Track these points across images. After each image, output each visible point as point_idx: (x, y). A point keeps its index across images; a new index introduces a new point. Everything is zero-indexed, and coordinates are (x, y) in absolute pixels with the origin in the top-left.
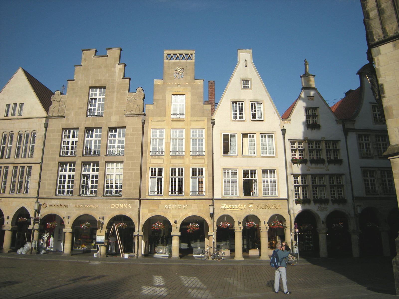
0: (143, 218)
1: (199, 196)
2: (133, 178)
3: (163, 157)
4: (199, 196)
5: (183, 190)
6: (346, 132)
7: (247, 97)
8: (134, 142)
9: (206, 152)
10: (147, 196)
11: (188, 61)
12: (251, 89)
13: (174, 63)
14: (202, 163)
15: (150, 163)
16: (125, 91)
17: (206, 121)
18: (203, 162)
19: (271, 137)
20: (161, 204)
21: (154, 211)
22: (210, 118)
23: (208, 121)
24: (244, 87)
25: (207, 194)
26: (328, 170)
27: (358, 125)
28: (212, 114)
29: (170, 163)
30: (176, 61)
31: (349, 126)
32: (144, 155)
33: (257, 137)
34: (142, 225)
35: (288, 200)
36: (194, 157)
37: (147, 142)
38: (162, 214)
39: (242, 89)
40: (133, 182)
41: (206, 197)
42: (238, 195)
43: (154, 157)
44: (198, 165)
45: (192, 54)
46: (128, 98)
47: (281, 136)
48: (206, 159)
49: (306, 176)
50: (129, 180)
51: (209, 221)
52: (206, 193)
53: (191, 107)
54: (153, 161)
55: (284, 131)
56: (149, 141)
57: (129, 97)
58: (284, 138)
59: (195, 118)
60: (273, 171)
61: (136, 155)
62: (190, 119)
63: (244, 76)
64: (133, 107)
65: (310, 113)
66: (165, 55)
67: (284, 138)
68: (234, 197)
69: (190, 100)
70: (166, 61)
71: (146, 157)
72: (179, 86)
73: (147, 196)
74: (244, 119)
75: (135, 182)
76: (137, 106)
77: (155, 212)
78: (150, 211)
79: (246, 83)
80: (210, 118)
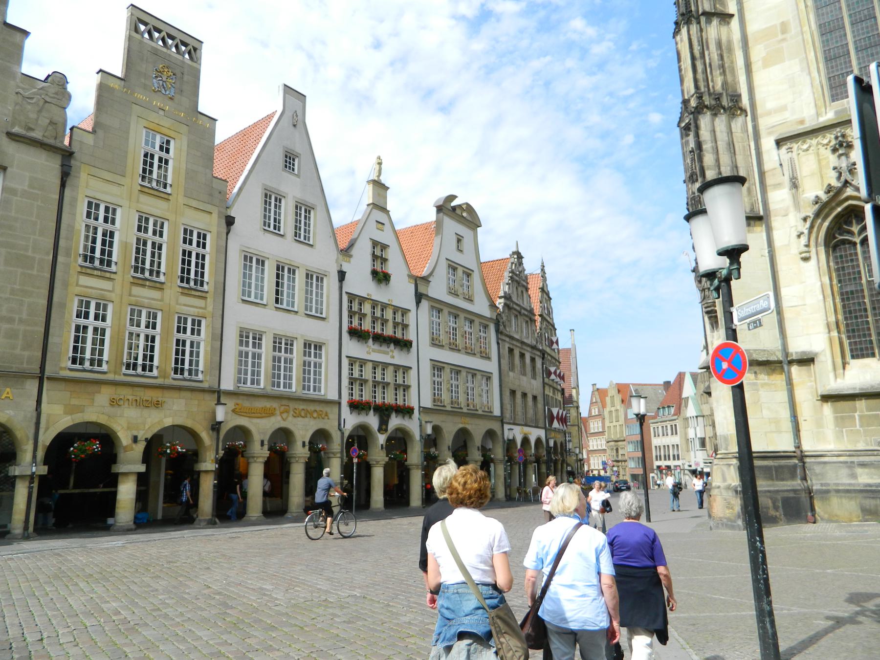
0: (47, 429)
1: (190, 380)
2: (24, 316)
3: (113, 276)
4: (190, 380)
5: (156, 362)
6: (419, 297)
8: (34, 219)
9: (212, 284)
10: (61, 369)
12: (298, 176)
14: (201, 308)
15: (77, 285)
16: (8, 64)
17: (215, 216)
18: (203, 306)
20: (99, 392)
21: (80, 409)
22: (223, 210)
23: (219, 217)
24: (286, 166)
25: (208, 378)
26: (393, 357)
29: (130, 295)
32: (60, 259)
33: (300, 277)
34: (43, 445)
35: (340, 404)
36: (186, 292)
37: (71, 228)
38: (102, 420)
40: (22, 328)
41: (205, 385)
42: (262, 386)
43: (89, 271)
44: (193, 311)
46: (18, 87)
48: (210, 300)
49: (365, 364)
50: (10, 320)
51: (206, 437)
52: (205, 376)
53: (187, 173)
54: (84, 280)
55: (342, 275)
56: (77, 226)
57: (23, 89)
58: (341, 288)
59: (194, 203)
60: (318, 347)
61: (37, 256)
62: (181, 200)
64: (37, 120)
65: (378, 252)
67: (341, 288)
68: (254, 388)
71: (67, 266)
72: (161, 112)
73: (61, 369)
75: (28, 328)
76: (48, 121)
77: (83, 412)
78: (70, 410)
80: (223, 210)
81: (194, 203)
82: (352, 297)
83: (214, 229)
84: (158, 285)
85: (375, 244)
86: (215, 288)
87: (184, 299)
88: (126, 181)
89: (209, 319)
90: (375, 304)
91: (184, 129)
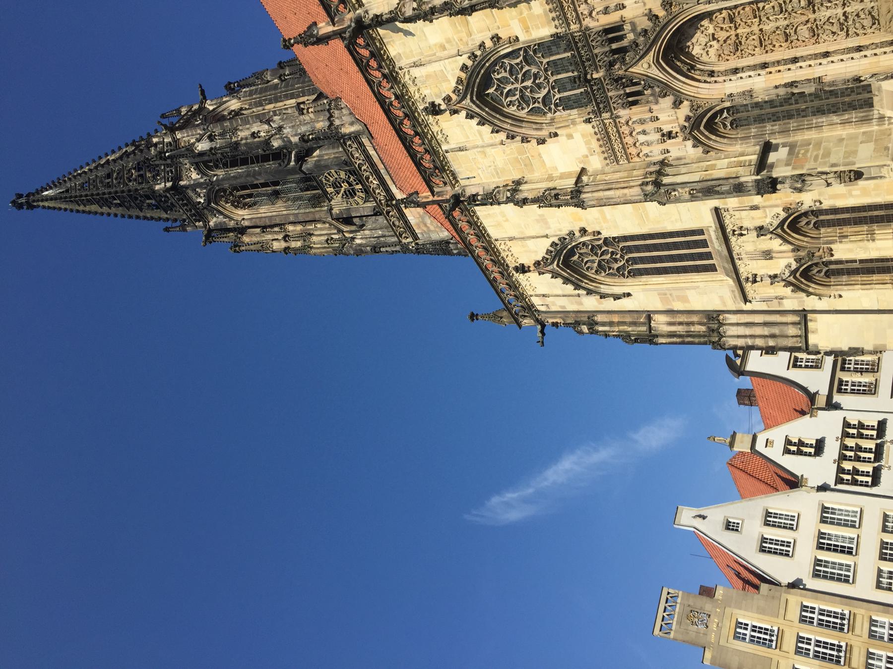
6: (831, 406)
7: (754, 529)
9: (843, 607)
11: (679, 600)
13: (679, 623)
19: (824, 509)
23: (789, 593)
24: (737, 530)
27: (824, 391)
28: (776, 584)
30: (675, 619)
31: (821, 401)
33: (827, 529)
39: (740, 532)
45: (668, 593)
47: (828, 493)
63: (721, 526)
66: (661, 634)
69: (746, 613)
70: (672, 635)
74: (792, 541)
79: (729, 526)
81: (782, 611)
82: (839, 480)
83: (800, 599)
84: (849, 648)
85: (787, 451)
86: (846, 605)
87: (857, 631)
88: (775, 659)
89: (871, 613)
90: (843, 458)
91: (728, 610)
